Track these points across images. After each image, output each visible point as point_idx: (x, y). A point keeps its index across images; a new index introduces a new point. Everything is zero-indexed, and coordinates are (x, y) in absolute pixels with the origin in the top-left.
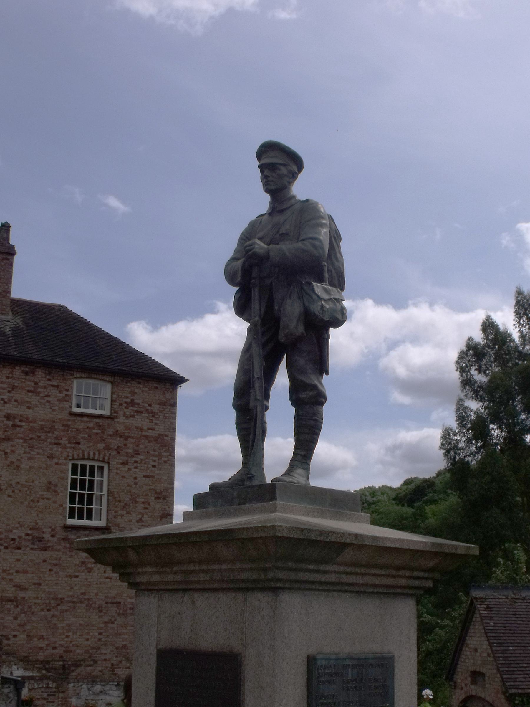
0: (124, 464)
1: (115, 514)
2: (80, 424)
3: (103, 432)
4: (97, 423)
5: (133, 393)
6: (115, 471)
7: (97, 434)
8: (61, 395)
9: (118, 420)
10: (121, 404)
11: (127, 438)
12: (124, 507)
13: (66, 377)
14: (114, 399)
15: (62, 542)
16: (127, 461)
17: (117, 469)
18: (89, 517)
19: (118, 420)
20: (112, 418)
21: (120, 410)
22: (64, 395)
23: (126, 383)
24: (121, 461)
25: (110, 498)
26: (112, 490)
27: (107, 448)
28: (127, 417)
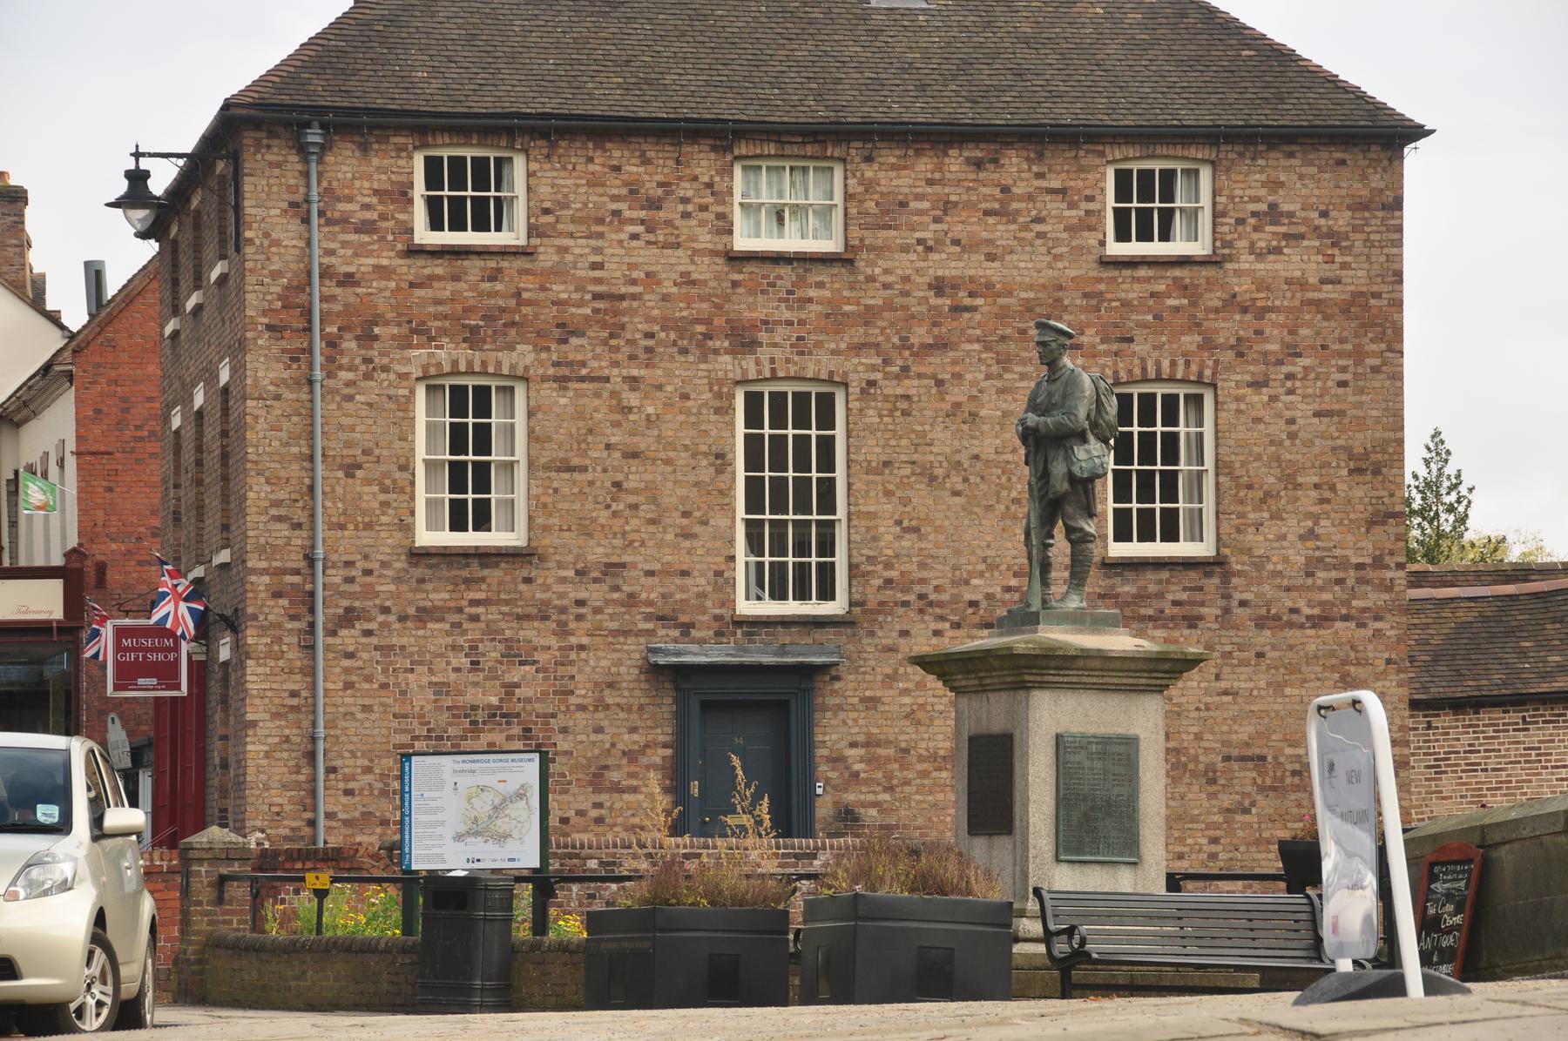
2: (1131, 288)
3: (1194, 304)
5: (1275, 185)
7: (1177, 309)
8: (1073, 213)
9: (1236, 266)
10: (1240, 221)
11: (1261, 313)
14: (1220, 208)
19: (1236, 266)
21: (1240, 238)
23: (1253, 159)
27: (1208, 345)
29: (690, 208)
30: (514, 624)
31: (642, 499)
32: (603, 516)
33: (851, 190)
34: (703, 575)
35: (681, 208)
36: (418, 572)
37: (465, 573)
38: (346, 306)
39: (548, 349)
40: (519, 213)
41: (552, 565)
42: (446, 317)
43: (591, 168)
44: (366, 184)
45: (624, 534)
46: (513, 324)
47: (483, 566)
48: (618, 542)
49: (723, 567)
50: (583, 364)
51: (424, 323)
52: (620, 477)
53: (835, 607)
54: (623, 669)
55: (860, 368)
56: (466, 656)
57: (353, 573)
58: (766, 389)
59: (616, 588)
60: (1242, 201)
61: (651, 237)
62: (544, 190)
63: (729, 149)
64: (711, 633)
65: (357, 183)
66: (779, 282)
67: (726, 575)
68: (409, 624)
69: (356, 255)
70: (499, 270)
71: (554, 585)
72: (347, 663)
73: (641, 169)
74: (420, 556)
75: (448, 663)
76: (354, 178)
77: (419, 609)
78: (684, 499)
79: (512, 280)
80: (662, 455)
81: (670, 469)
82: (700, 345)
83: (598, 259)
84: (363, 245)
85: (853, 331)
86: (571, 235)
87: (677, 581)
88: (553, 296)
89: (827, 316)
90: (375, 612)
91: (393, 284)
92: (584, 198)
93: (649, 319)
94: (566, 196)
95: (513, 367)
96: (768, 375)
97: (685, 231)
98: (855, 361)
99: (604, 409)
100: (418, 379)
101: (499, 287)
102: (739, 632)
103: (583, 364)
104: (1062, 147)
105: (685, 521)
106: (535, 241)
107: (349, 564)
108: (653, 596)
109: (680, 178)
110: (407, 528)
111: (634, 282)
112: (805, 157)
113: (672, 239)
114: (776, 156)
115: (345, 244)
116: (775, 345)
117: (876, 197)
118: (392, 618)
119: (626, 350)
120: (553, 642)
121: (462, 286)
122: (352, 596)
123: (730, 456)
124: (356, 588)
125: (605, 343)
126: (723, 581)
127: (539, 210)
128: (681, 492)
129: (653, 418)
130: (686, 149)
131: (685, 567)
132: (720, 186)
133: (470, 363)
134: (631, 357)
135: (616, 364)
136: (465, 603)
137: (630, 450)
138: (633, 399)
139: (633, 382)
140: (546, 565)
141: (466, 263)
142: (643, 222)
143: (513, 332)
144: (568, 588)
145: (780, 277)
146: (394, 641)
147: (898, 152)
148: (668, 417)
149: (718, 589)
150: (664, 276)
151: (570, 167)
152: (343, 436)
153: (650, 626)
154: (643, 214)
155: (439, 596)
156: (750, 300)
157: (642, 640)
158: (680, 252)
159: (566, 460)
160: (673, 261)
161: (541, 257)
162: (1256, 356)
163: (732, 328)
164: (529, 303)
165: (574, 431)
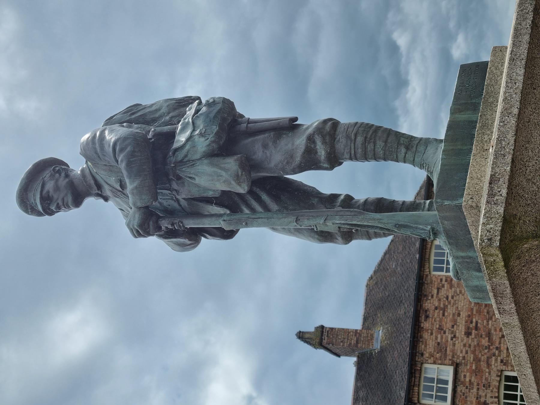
8: (446, 286)
33: (432, 362)
55: (496, 365)
66: (463, 391)
85: (482, 366)
89: (476, 375)
96: (497, 400)
98: (493, 366)
112: (420, 377)
116: (486, 395)
145: (461, 391)
147: (421, 344)
156: (469, 403)
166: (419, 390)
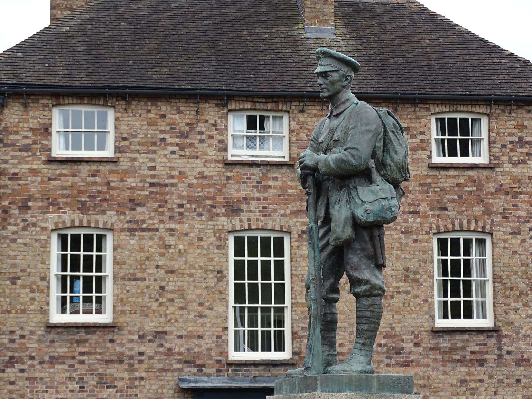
0: (515, 233)
1: (505, 308)
2: (445, 181)
3: (480, 190)
4: (469, 176)
5: (522, 127)
6: (502, 245)
7: (470, 192)
8: (414, 140)
9: (502, 170)
10: (504, 146)
11: (516, 195)
12: (519, 296)
13: (418, 114)
14: (492, 138)
15: (431, 352)
16: (519, 228)
17: (505, 241)
18: (468, 315)
19: (502, 170)
20: (491, 168)
21: (503, 155)
22: (418, 141)
23: (510, 113)
24: (509, 230)
25: (496, 284)
26: (499, 274)
27: (488, 212)
28: (514, 164)
29: (204, 137)
30: (104, 365)
31: (176, 296)
32: (155, 306)
33: (292, 128)
34: (210, 337)
35: (199, 137)
36: (51, 337)
37: (77, 337)
38: (13, 191)
39: (125, 214)
40: (111, 141)
41: (125, 332)
42: (68, 196)
43: (149, 115)
44: (26, 125)
45: (166, 315)
46: (105, 200)
47: (87, 333)
48: (162, 320)
49: (221, 334)
50: (144, 222)
51: (56, 200)
52: (164, 284)
53: (285, 355)
54: (165, 391)
55: (298, 224)
56: (77, 383)
57: (15, 337)
58: (246, 235)
59: (161, 345)
60: (504, 136)
61: (183, 153)
62: (124, 128)
63: (225, 105)
64: (214, 370)
65: (21, 125)
66: (253, 177)
67: (223, 338)
68: (45, 365)
69: (19, 163)
70: (98, 171)
71: (126, 343)
72: (10, 387)
73: (177, 116)
74: (52, 327)
75: (67, 387)
76: (19, 122)
77: (51, 357)
78: (199, 296)
79: (105, 176)
80: (188, 272)
81: (192, 279)
82: (209, 211)
83: (153, 164)
84: (24, 158)
85: (294, 203)
86: (138, 152)
87: (196, 341)
88: (127, 185)
89: (280, 195)
90: (26, 359)
91: (39, 179)
92: (145, 132)
93: (181, 197)
94: (135, 131)
95: (105, 223)
96: (247, 228)
97: (201, 149)
98: (295, 220)
99: (155, 246)
100: (52, 230)
101: (98, 180)
102: (230, 370)
103: (144, 222)
104: (407, 105)
105: (200, 308)
106: (119, 155)
107: (12, 332)
108: (182, 350)
109: (198, 121)
110: (45, 312)
111: (172, 177)
112: (267, 110)
113: (194, 154)
114: (251, 110)
115: (13, 157)
116: (251, 211)
117: (306, 131)
118: (36, 362)
119: (168, 214)
120: (126, 375)
121: (77, 179)
122: (14, 350)
123: (225, 272)
124: (16, 345)
125: (156, 210)
126: (220, 340)
127: (121, 138)
128: (198, 292)
129: (183, 251)
130: (202, 105)
131: (200, 334)
132: (221, 125)
133: (81, 221)
134: (171, 218)
135: (162, 222)
136: (76, 354)
137: (170, 269)
138: (171, 241)
139: (172, 231)
140: (122, 333)
141: (80, 167)
142: (178, 145)
143: (105, 204)
144: (134, 345)
145: (253, 174)
146: (37, 375)
147: (318, 108)
148: (191, 251)
149: (218, 345)
150: (189, 173)
151: (138, 115)
152: (10, 262)
153: (180, 366)
154: (178, 140)
155: (62, 350)
156: (237, 186)
157: (176, 374)
158: (198, 161)
159: (133, 274)
160: (194, 165)
161: (121, 164)
162: (513, 218)
163: (227, 202)
164: (114, 188)
165: (138, 258)
166: (247, 110)
